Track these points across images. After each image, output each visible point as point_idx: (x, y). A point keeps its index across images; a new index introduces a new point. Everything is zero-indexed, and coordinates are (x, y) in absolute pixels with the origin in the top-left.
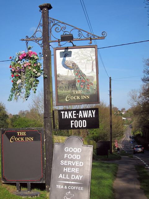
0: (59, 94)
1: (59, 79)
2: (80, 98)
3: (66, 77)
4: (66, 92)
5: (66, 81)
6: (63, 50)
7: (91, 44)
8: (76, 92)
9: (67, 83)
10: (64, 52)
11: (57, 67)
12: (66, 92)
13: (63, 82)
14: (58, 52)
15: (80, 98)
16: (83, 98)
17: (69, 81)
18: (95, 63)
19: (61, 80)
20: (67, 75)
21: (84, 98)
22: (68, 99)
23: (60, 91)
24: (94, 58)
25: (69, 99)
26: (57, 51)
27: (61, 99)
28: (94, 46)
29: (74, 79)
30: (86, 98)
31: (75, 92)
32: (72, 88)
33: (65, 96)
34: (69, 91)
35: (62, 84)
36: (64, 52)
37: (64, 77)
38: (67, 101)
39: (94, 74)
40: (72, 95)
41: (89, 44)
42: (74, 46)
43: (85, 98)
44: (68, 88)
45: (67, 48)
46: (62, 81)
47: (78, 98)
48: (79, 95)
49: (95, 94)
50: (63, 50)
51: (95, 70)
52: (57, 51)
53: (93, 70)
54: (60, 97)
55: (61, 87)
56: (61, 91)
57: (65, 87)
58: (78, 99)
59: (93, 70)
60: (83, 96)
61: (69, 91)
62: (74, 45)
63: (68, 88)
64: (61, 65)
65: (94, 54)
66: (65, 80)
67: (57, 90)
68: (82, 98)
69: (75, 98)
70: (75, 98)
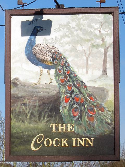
0: (14, 131)
1: (17, 93)
2: (70, 143)
3: (34, 86)
4: (32, 126)
5: (34, 98)
6: (31, 18)
7: (103, 5)
8: (60, 128)
9: (37, 104)
10: (31, 23)
11: (13, 61)
12: (32, 126)
13: (26, 101)
14: (17, 21)
15: (70, 143)
16: (76, 144)
17: (42, 99)
18: (111, 53)
19: (20, 95)
20: (36, 82)
21: (80, 144)
22: (36, 145)
23: (17, 124)
24: (110, 40)
25: (39, 144)
26: (13, 17)
27: (19, 144)
28: (110, 10)
29: (54, 93)
30: (85, 144)
31: (57, 128)
32: (50, 116)
33: (29, 136)
34: (42, 125)
35: (24, 104)
36: (33, 21)
37: (30, 89)
38: (34, 149)
39: (109, 82)
40: (48, 134)
41: (98, 5)
42: (58, 6)
43: (83, 144)
44: (40, 117)
45: (40, 13)
46: (22, 97)
47: (64, 143)
48: (66, 135)
49: (109, 136)
50: (31, 18)
51: (111, 73)
52: (14, 18)
53: (105, 71)
54: (17, 138)
55: (20, 112)
56: (20, 123)
57: (32, 114)
58: (63, 145)
59: (105, 71)
60: (76, 141)
61: (42, 125)
62: (60, 4)
63: (40, 117)
64: (24, 56)
65: (110, 31)
66: (32, 96)
67: (10, 119)
68: (74, 145)
69: (57, 142)
70: (57, 144)
